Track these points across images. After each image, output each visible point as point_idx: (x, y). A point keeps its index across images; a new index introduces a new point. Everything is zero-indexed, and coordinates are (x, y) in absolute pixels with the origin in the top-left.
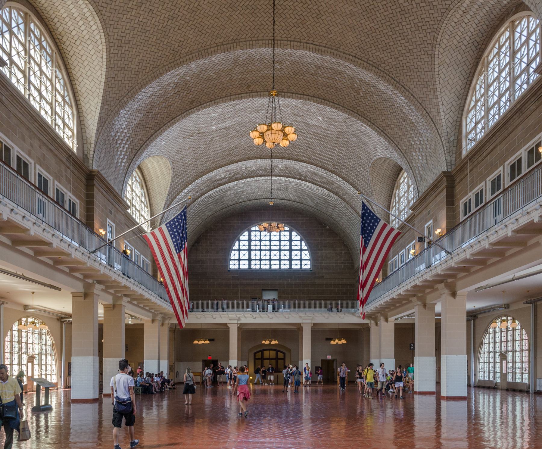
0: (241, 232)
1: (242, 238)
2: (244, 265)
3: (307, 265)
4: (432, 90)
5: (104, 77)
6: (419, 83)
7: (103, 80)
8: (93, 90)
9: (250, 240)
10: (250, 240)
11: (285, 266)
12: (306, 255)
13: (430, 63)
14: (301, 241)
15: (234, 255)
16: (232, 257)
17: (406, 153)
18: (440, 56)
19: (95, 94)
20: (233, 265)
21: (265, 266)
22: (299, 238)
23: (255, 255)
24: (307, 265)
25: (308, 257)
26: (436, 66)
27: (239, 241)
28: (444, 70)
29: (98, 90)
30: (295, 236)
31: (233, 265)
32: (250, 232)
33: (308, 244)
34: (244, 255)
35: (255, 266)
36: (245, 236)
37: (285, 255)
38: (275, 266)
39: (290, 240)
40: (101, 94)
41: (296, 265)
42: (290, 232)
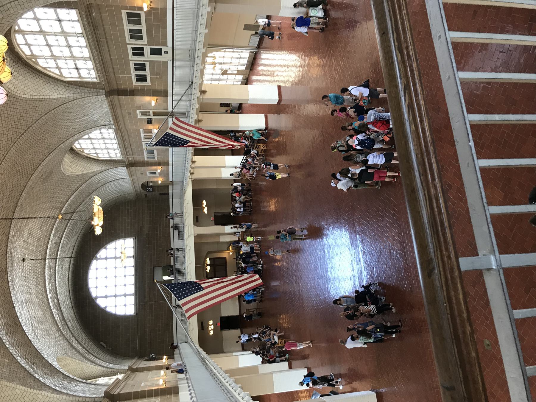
0: (97, 306)
2: (131, 300)
4: (40, 103)
5: (21, 387)
6: (31, 113)
7: (24, 388)
8: (32, 399)
9: (106, 297)
10: (106, 297)
11: (131, 262)
13: (21, 101)
14: (106, 248)
17: (71, 135)
18: (19, 92)
19: (34, 396)
21: (131, 280)
23: (120, 291)
26: (25, 96)
27: (106, 307)
28: (28, 91)
29: (32, 394)
30: (102, 253)
32: (97, 298)
34: (120, 300)
35: (131, 289)
36: (101, 303)
38: (131, 271)
39: (106, 258)
40: (35, 391)
41: (131, 252)
42: (97, 259)
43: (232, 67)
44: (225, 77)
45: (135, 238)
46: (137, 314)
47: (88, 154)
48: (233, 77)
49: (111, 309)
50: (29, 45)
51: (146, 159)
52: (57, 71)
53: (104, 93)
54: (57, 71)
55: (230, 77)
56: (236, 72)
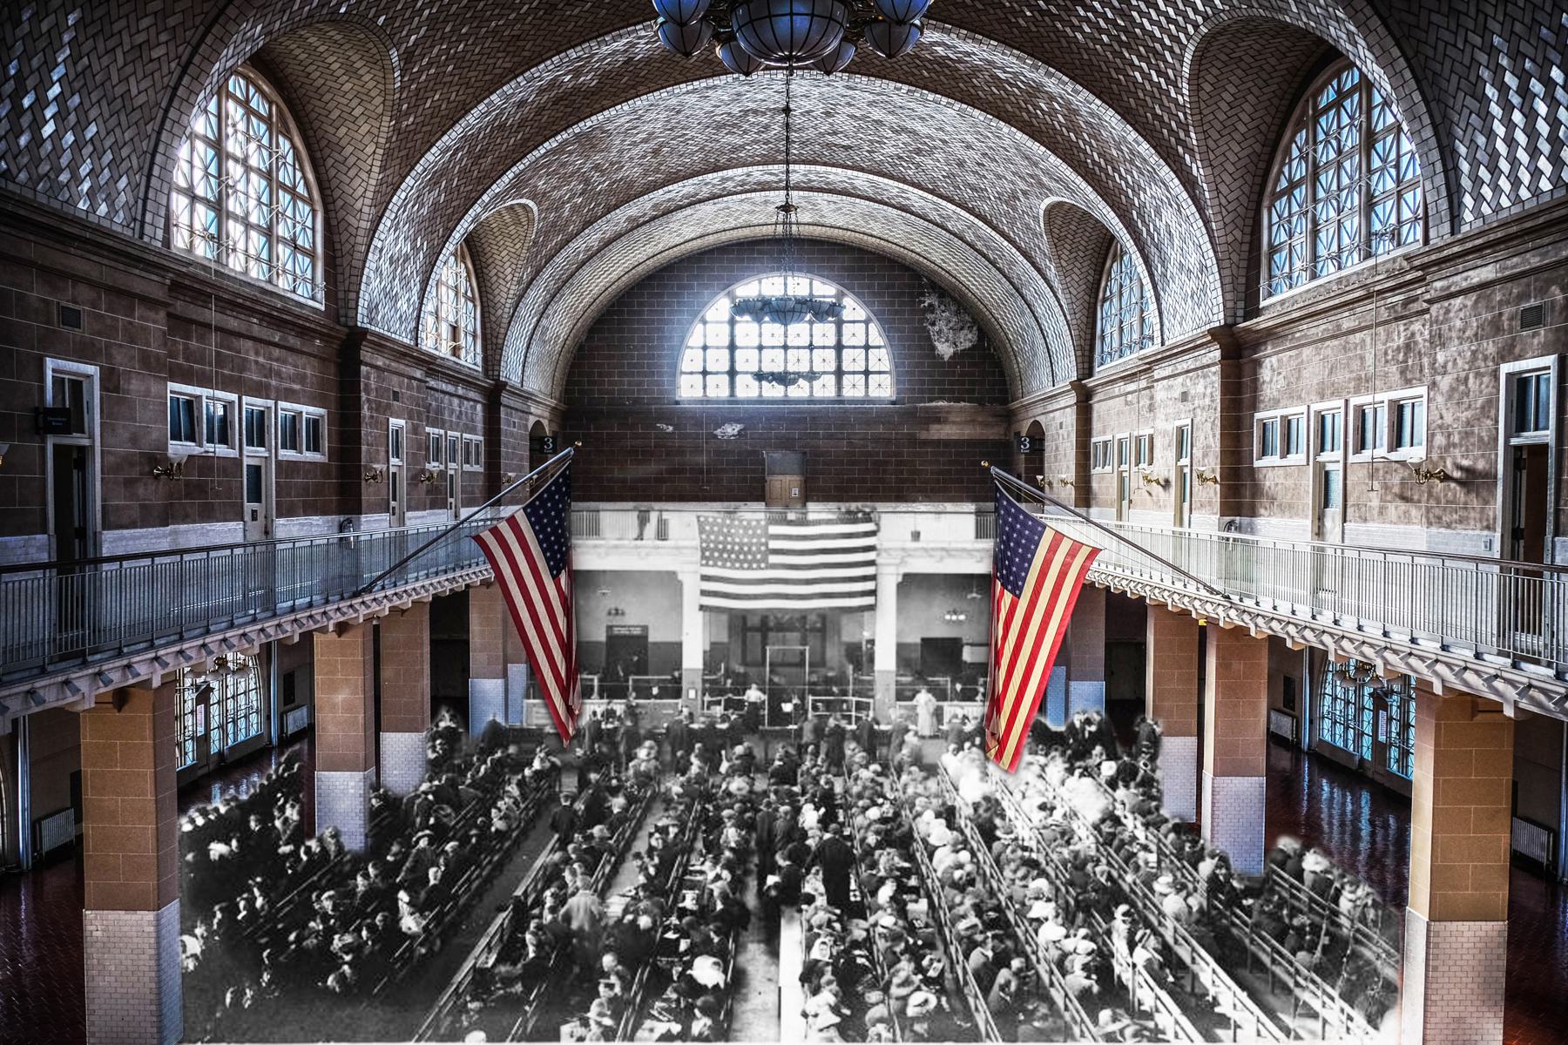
1: (710, 314)
3: (883, 389)
12: (882, 359)
14: (867, 322)
15: (690, 360)
16: (685, 366)
20: (688, 389)
22: (861, 313)
24: (883, 389)
25: (886, 365)
27: (705, 323)
31: (688, 389)
33: (888, 329)
36: (720, 308)
37: (825, 360)
41: (853, 389)
43: (1395, 727)
44: (1368, 702)
45: (893, 403)
46: (677, 403)
47: (1109, 274)
48: (1368, 729)
49: (696, 336)
50: (1337, 104)
51: (1094, 440)
52: (1284, 184)
53: (1230, 320)
54: (1284, 184)
55: (1368, 716)
56: (1382, 738)
